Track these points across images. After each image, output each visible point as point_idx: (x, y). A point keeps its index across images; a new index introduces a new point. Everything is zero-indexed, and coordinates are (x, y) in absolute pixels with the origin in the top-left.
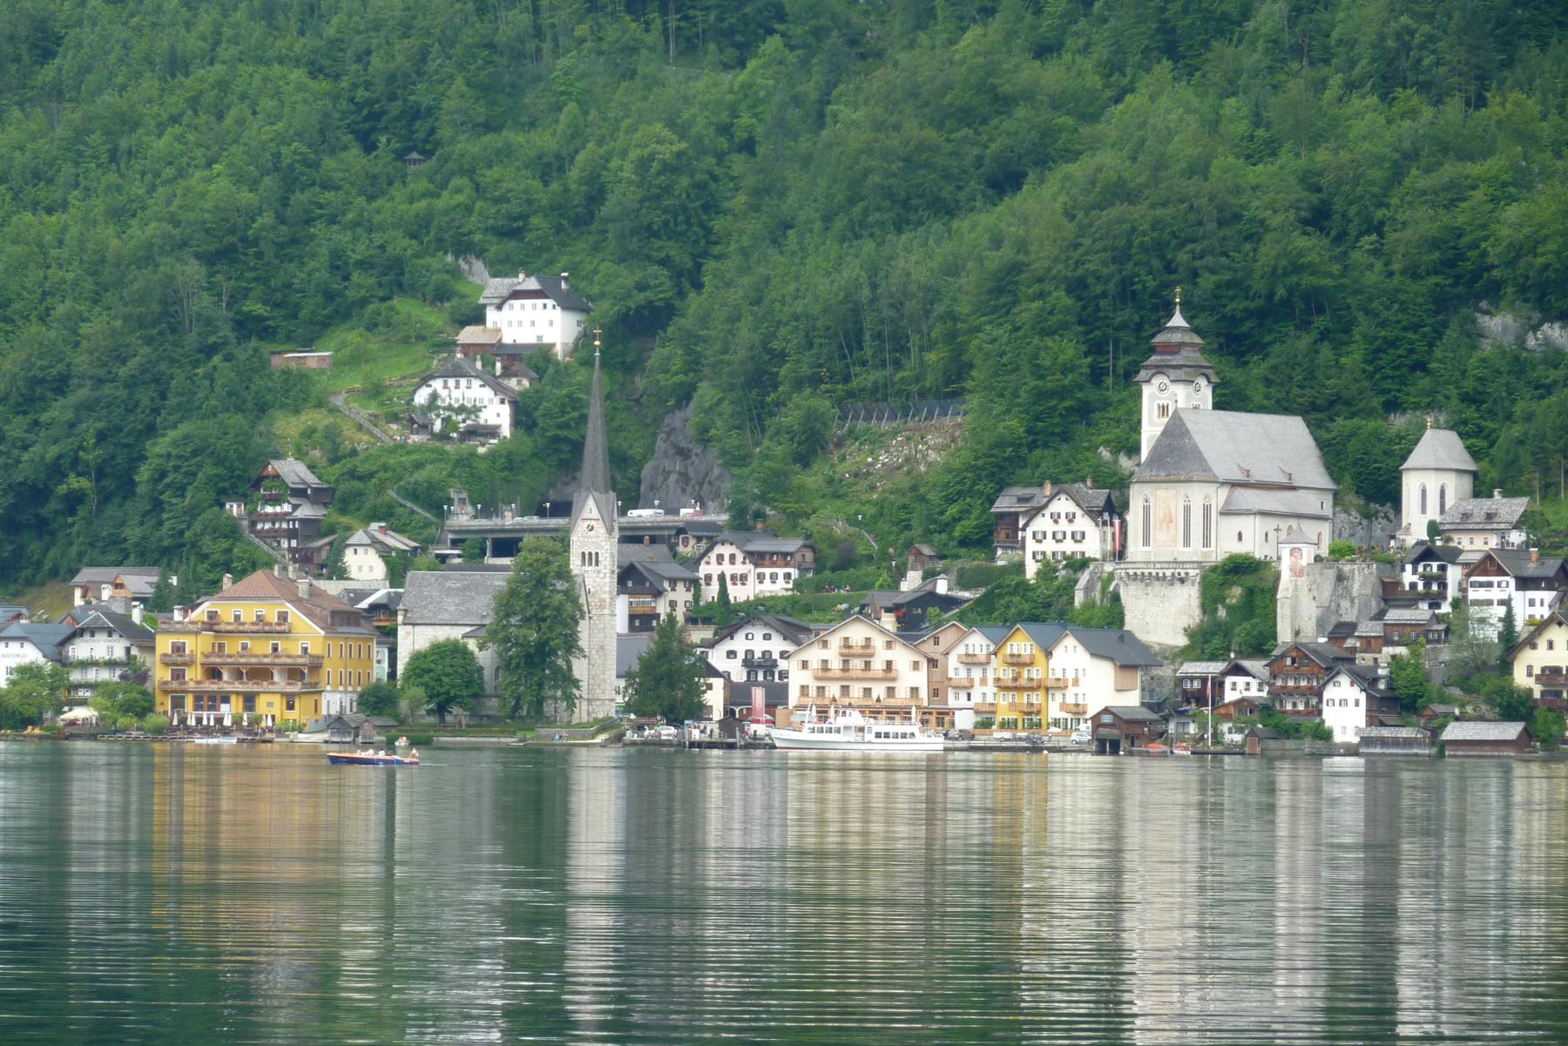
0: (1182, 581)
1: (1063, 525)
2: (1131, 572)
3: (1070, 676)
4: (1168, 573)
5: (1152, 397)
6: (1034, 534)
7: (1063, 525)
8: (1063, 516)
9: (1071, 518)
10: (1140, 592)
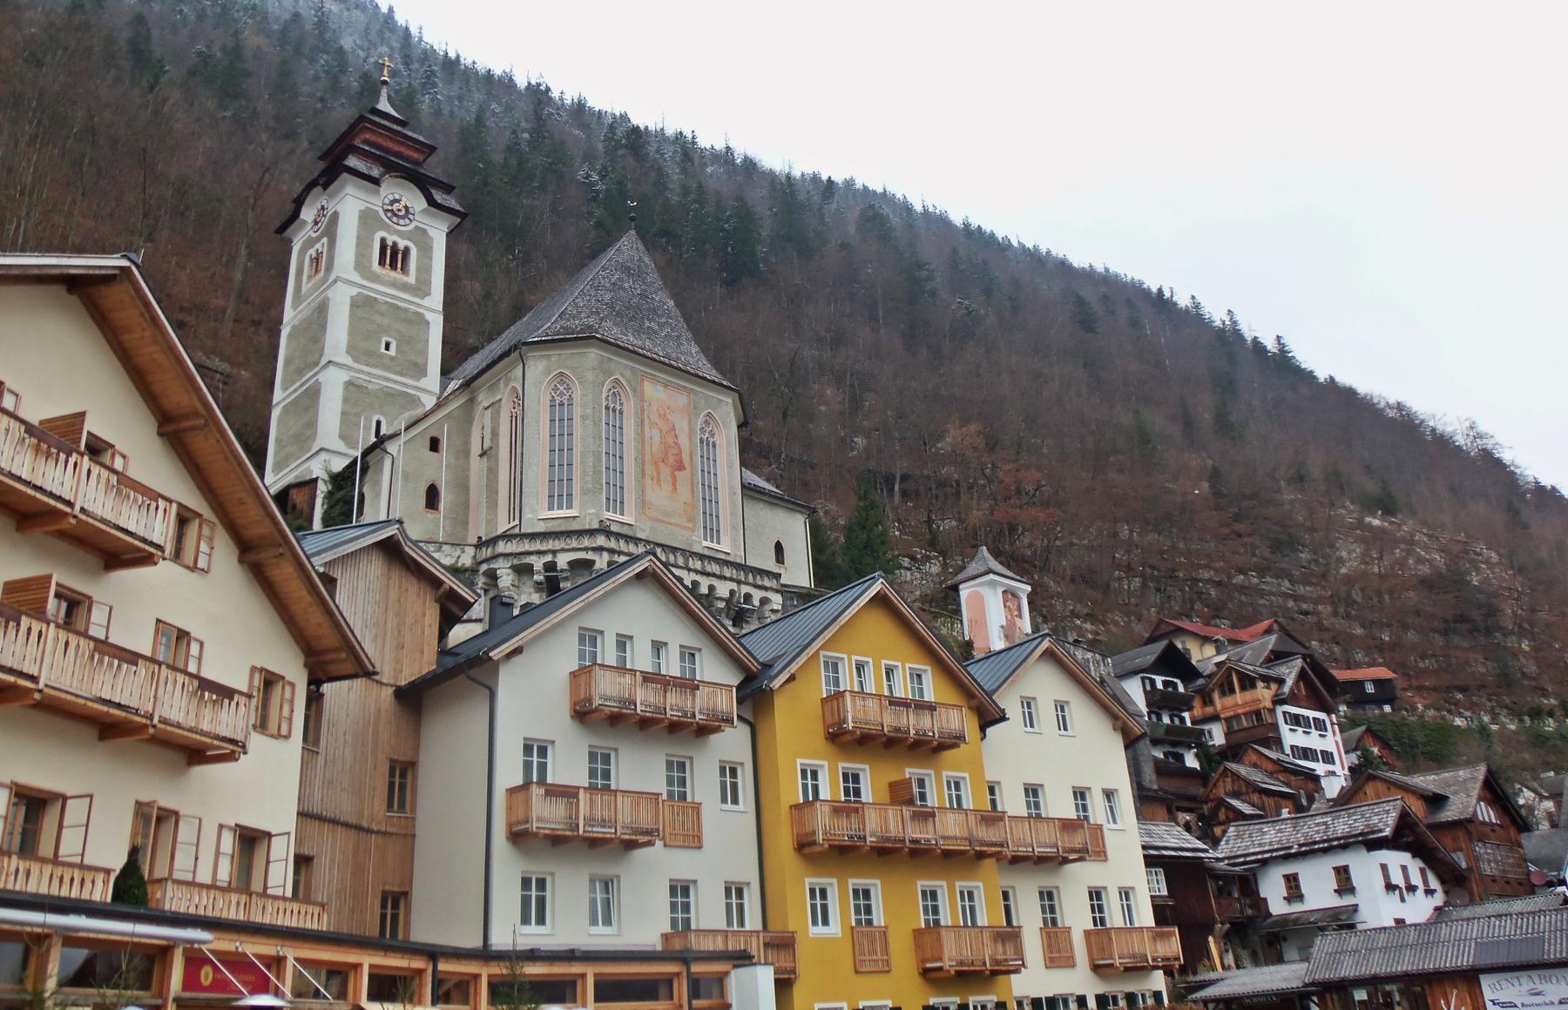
4: (723, 589)
5: (367, 220)
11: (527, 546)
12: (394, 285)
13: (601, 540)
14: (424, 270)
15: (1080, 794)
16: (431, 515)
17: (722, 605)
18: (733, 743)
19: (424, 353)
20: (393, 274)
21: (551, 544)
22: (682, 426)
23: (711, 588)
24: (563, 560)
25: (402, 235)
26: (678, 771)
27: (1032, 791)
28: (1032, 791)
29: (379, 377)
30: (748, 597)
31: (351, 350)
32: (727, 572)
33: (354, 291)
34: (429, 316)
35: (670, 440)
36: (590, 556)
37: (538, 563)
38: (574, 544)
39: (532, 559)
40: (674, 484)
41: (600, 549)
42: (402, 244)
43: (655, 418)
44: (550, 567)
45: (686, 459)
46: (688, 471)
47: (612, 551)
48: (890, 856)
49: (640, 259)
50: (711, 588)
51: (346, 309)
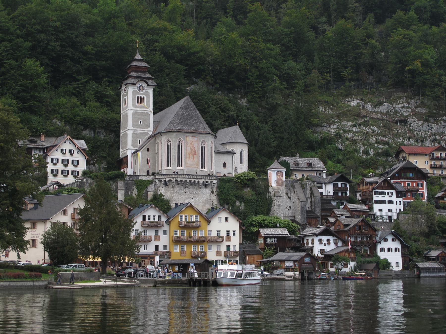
0: (206, 186)
1: (67, 156)
2: (179, 180)
3: (223, 234)
4: (201, 181)
5: (134, 93)
6: (52, 160)
7: (67, 156)
8: (67, 151)
9: (71, 153)
10: (181, 191)
11: (161, 177)
12: (141, 107)
13: (173, 176)
14: (148, 101)
15: (228, 232)
16: (148, 165)
17: (201, 184)
18: (166, 227)
19: (149, 122)
20: (141, 105)
21: (165, 177)
22: (196, 145)
23: (198, 181)
24: (167, 180)
25: (142, 94)
26: (157, 232)
27: (218, 232)
28: (218, 232)
29: (139, 130)
30: (207, 182)
31: (133, 126)
32: (202, 177)
33: (132, 111)
34: (149, 113)
35: (193, 149)
36: (171, 179)
37: (163, 180)
38: (169, 177)
39: (162, 179)
40: (193, 158)
41: (173, 178)
42: (142, 97)
43: (189, 144)
44: (165, 181)
45: (197, 152)
46: (197, 155)
47: (176, 178)
48: (188, 242)
49: (190, 104)
50: (198, 181)
51: (131, 116)
